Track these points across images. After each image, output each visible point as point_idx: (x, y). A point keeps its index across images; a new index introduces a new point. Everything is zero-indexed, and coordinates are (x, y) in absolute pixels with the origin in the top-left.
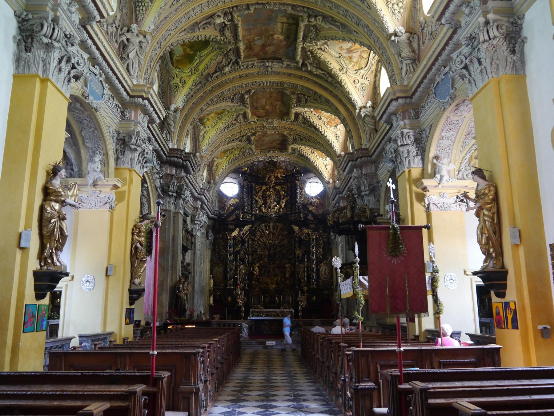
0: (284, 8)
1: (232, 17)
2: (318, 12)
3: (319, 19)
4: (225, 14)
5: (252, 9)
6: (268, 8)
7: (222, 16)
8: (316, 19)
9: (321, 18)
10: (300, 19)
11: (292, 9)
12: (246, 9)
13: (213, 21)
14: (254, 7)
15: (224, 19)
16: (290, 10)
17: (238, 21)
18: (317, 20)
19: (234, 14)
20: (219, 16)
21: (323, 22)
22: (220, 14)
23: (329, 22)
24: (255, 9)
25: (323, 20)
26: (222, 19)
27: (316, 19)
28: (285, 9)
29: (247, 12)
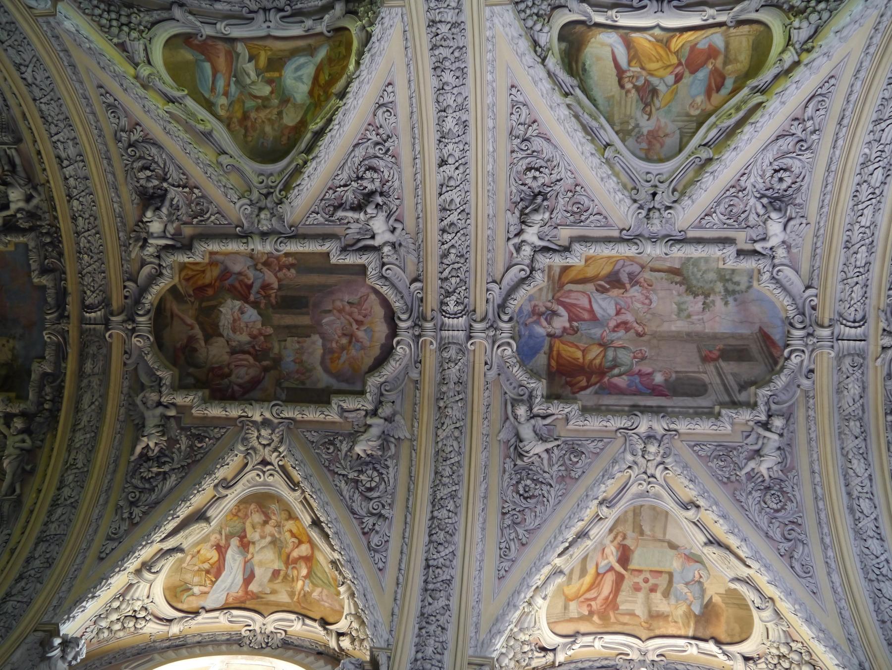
0: (49, 354)
1: (24, 231)
2: (41, 437)
3: (23, 441)
4: (31, 215)
5: (45, 280)
6: (48, 317)
7: (30, 206)
8: (22, 432)
9: (28, 444)
10: (13, 395)
11: (45, 375)
12: (42, 265)
13: (22, 182)
14: (50, 284)
15: (19, 210)
16: (39, 369)
17: (6, 245)
18: (20, 437)
19: (33, 235)
20: (28, 199)
21: (18, 452)
22: (35, 202)
23: (18, 466)
24: (43, 288)
25: (22, 449)
26: (21, 204)
27: (22, 432)
28: (44, 358)
29: (34, 266)
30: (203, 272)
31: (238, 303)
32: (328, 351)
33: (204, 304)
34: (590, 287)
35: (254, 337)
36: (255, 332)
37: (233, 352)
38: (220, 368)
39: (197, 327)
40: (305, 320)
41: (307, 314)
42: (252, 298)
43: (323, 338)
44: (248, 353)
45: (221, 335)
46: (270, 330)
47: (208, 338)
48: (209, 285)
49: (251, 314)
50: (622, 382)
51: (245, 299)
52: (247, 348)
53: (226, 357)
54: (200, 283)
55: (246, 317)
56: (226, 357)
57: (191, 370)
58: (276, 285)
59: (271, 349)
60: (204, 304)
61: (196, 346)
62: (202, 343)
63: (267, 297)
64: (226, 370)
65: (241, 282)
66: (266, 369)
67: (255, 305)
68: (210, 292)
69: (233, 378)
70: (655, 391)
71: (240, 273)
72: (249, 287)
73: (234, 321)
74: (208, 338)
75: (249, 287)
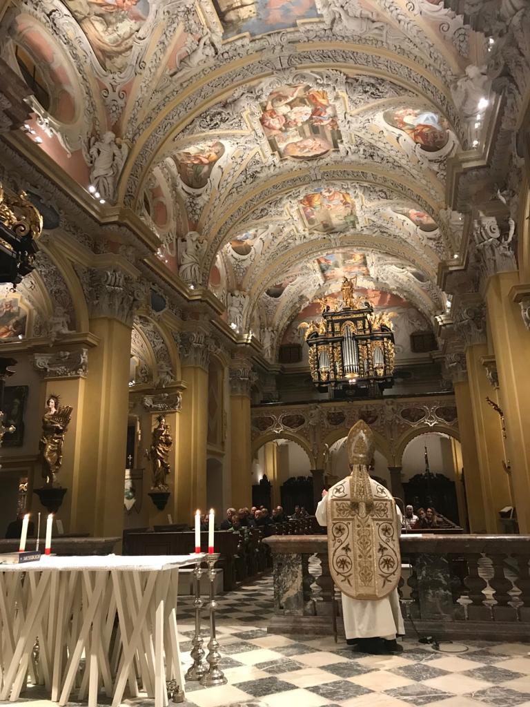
30: (324, 98)
31: (310, 112)
32: (296, 144)
33: (306, 100)
34: (342, 199)
35: (295, 121)
36: (297, 121)
37: (284, 116)
38: (275, 113)
39: (293, 98)
40: (308, 134)
41: (311, 133)
42: (314, 117)
43: (301, 141)
44: (286, 121)
45: (292, 109)
46: (300, 125)
47: (289, 104)
48: (316, 100)
49: (307, 118)
50: (309, 210)
51: (314, 113)
52: (289, 120)
53: (280, 114)
54: (317, 97)
55: (303, 116)
56: (280, 114)
57: (270, 103)
58: (322, 124)
59: (291, 127)
60: (306, 100)
61: (283, 101)
62: (286, 102)
63: (316, 122)
64: (275, 116)
65: (322, 113)
66: (280, 129)
67: (311, 118)
68: (314, 101)
69: (272, 120)
70: (308, 217)
71: (325, 112)
72: (320, 115)
73: (300, 112)
74: (289, 104)
75: (320, 115)
